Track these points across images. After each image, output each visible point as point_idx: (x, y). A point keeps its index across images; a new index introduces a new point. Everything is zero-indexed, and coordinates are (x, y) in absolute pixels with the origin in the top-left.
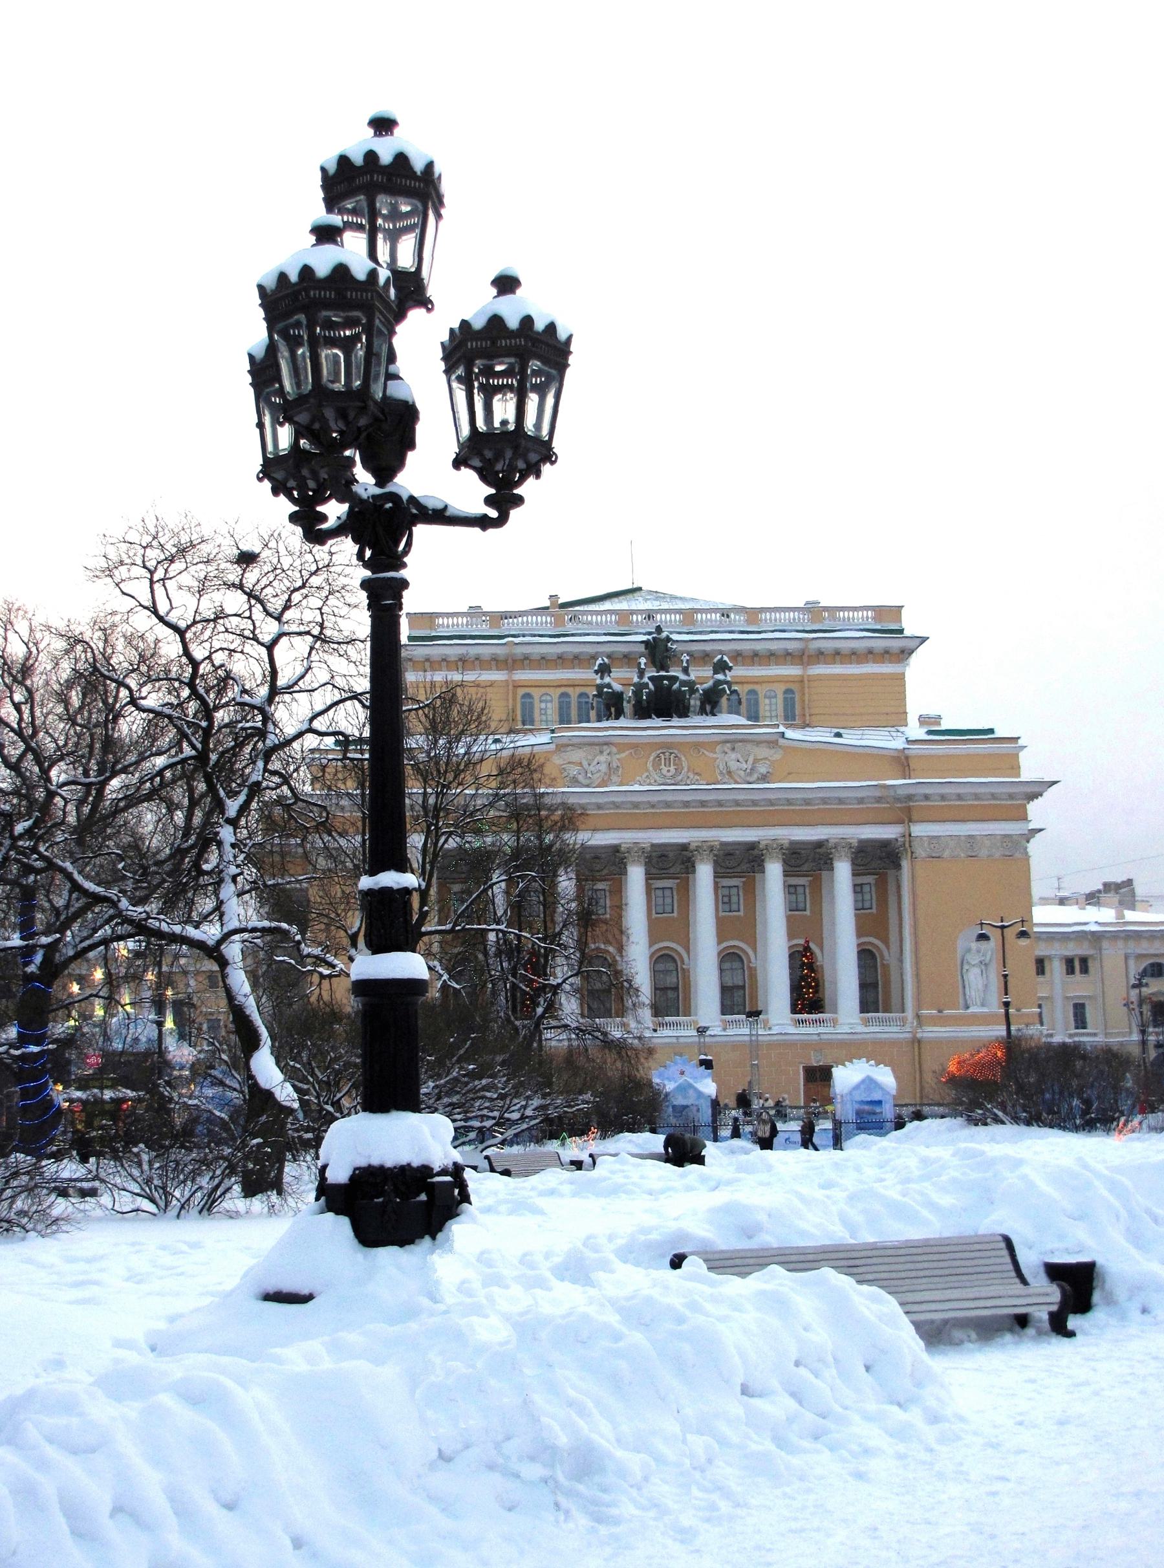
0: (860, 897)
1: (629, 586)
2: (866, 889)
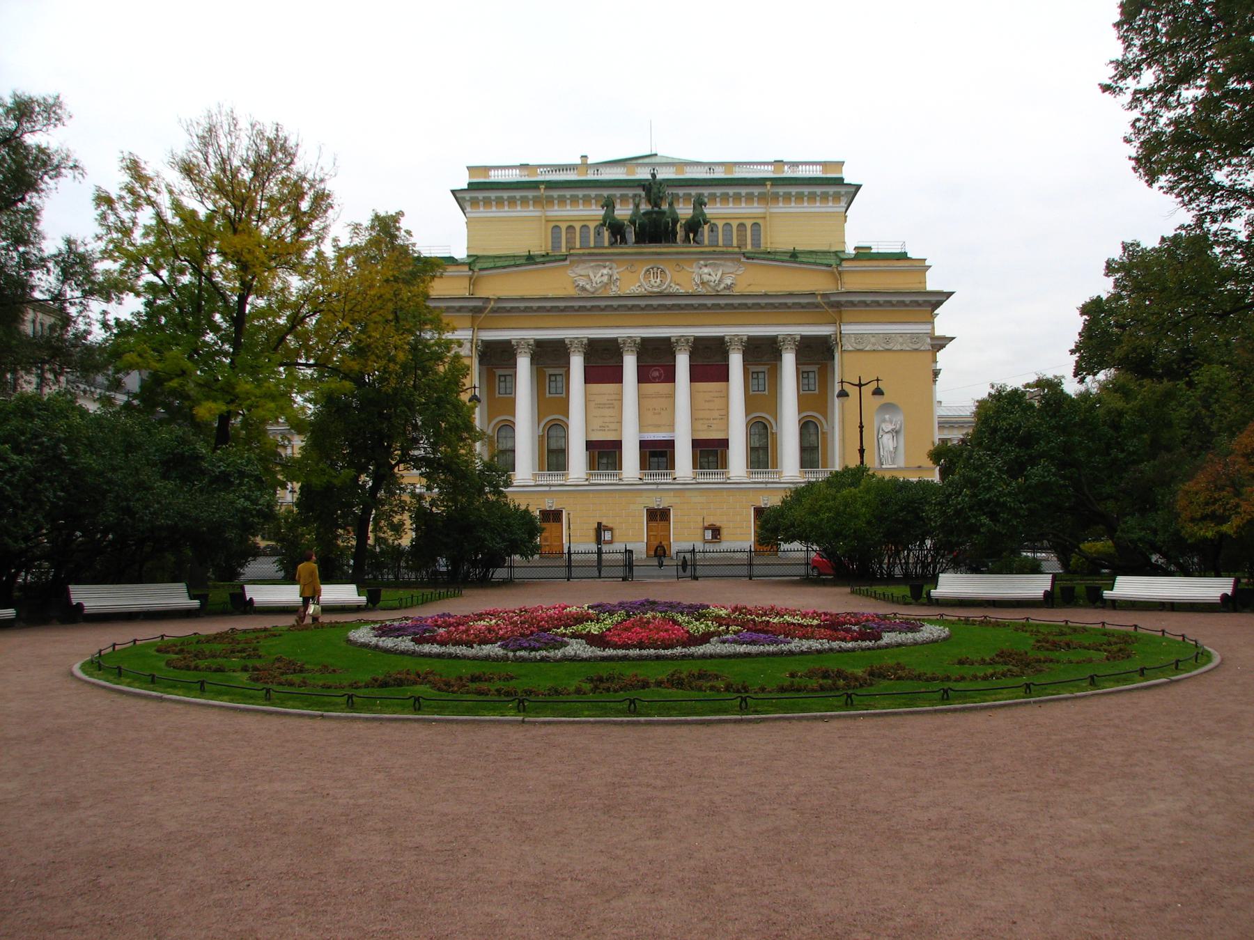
0: (806, 381)
1: (649, 153)
2: (811, 375)
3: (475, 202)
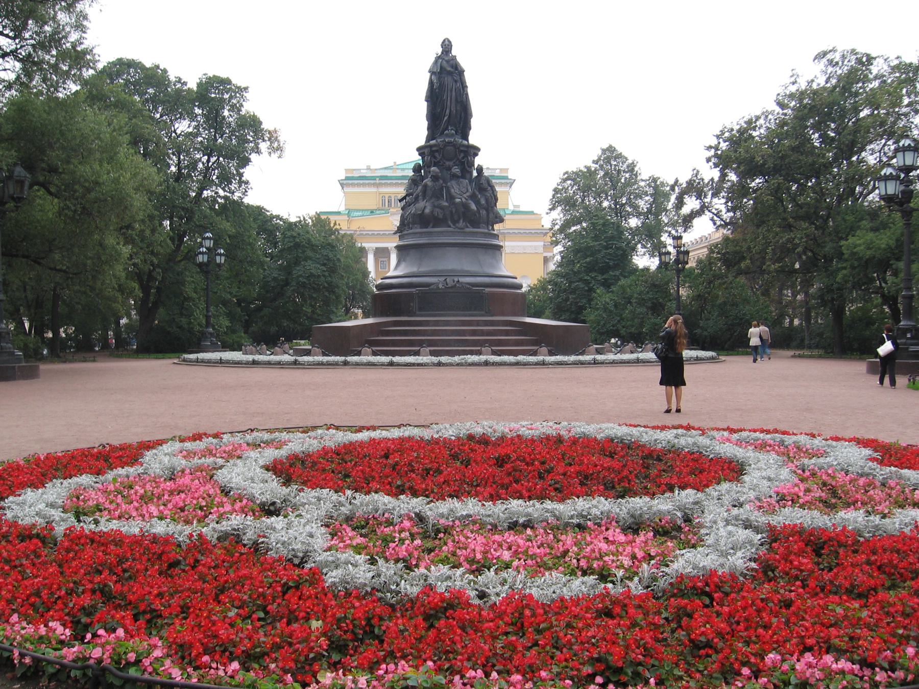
3: (348, 185)
